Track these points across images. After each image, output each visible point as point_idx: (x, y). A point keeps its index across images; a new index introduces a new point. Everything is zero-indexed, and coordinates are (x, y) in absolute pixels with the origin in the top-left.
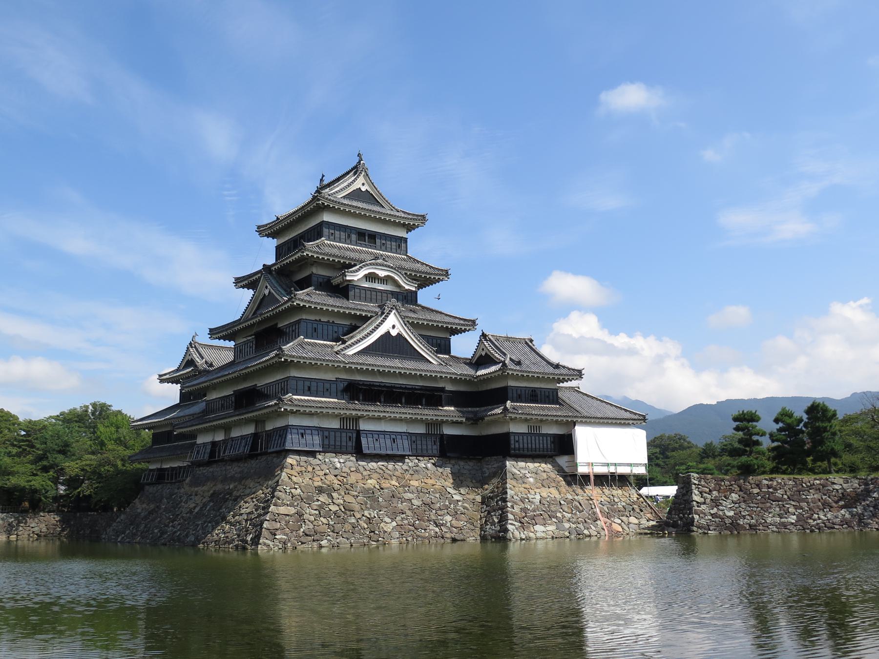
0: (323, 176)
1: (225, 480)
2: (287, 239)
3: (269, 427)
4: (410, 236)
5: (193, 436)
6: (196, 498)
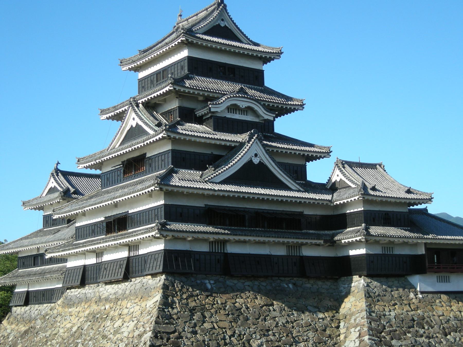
4: (267, 68)
5: (63, 260)
6: (72, 318)
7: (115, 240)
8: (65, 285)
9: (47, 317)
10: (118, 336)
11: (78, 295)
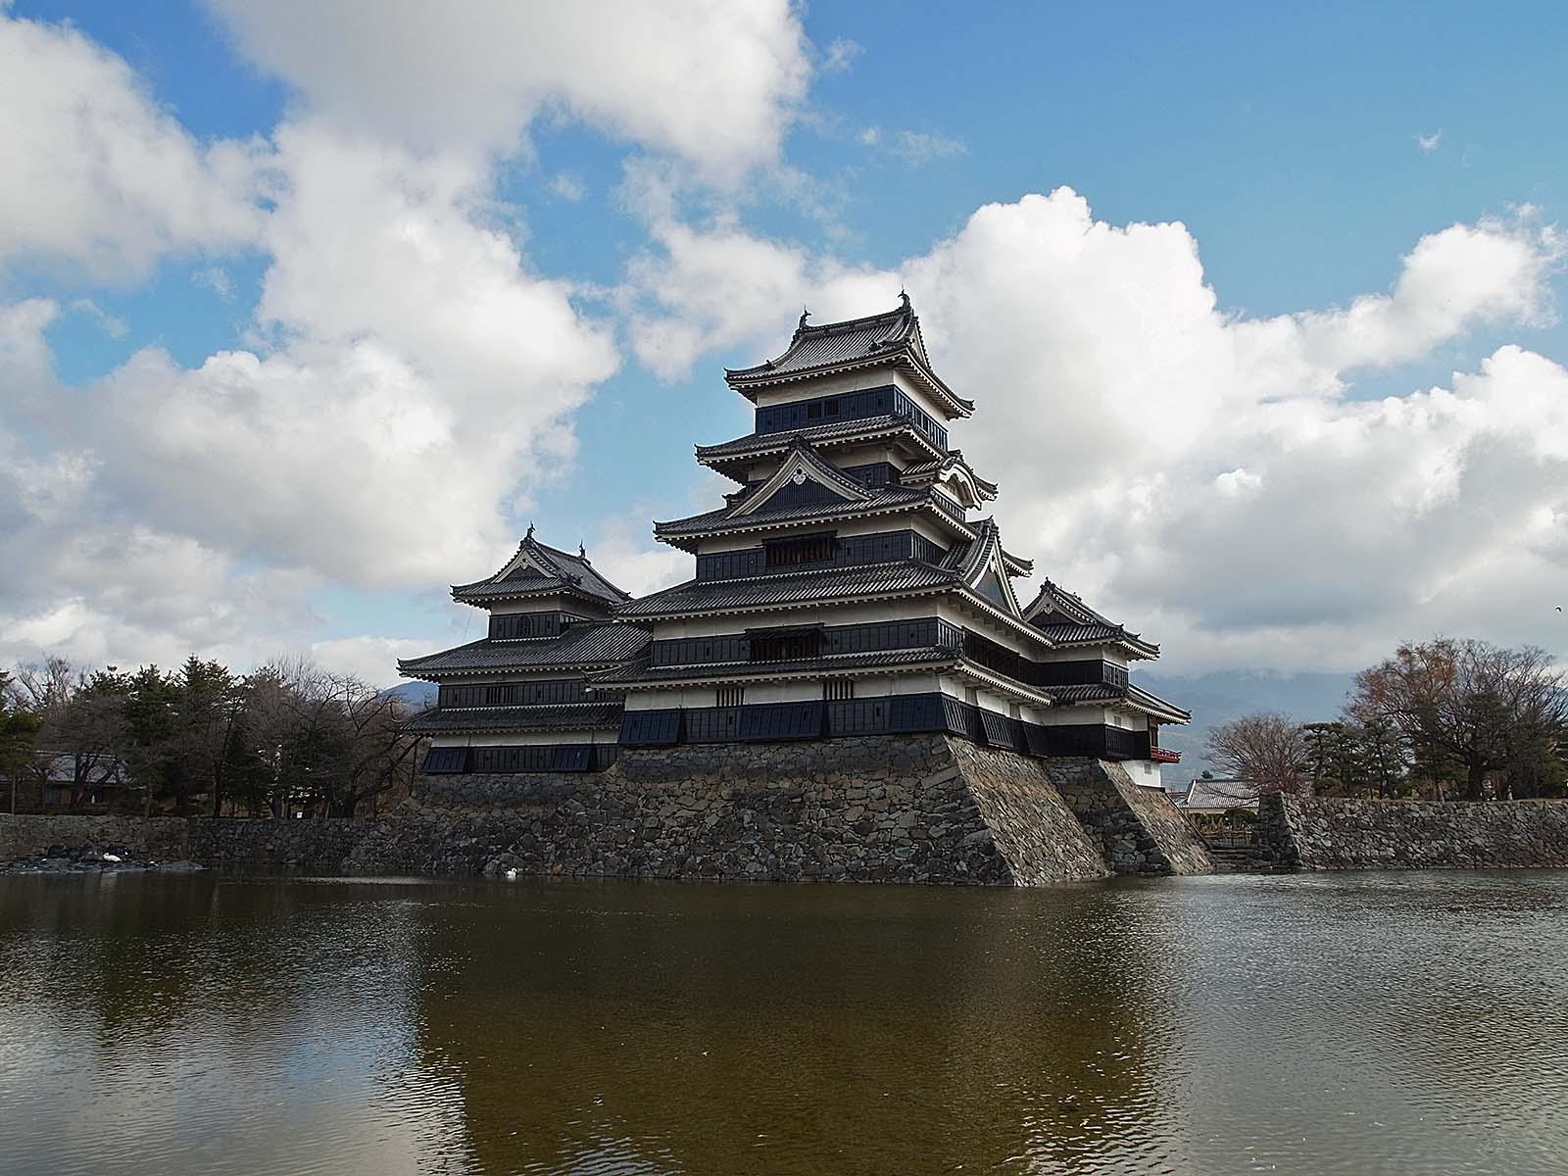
0: (806, 314)
1: (745, 773)
2: (789, 401)
3: (863, 692)
4: (951, 426)
5: (623, 695)
7: (820, 670)
9: (598, 797)
10: (873, 835)
11: (669, 761)
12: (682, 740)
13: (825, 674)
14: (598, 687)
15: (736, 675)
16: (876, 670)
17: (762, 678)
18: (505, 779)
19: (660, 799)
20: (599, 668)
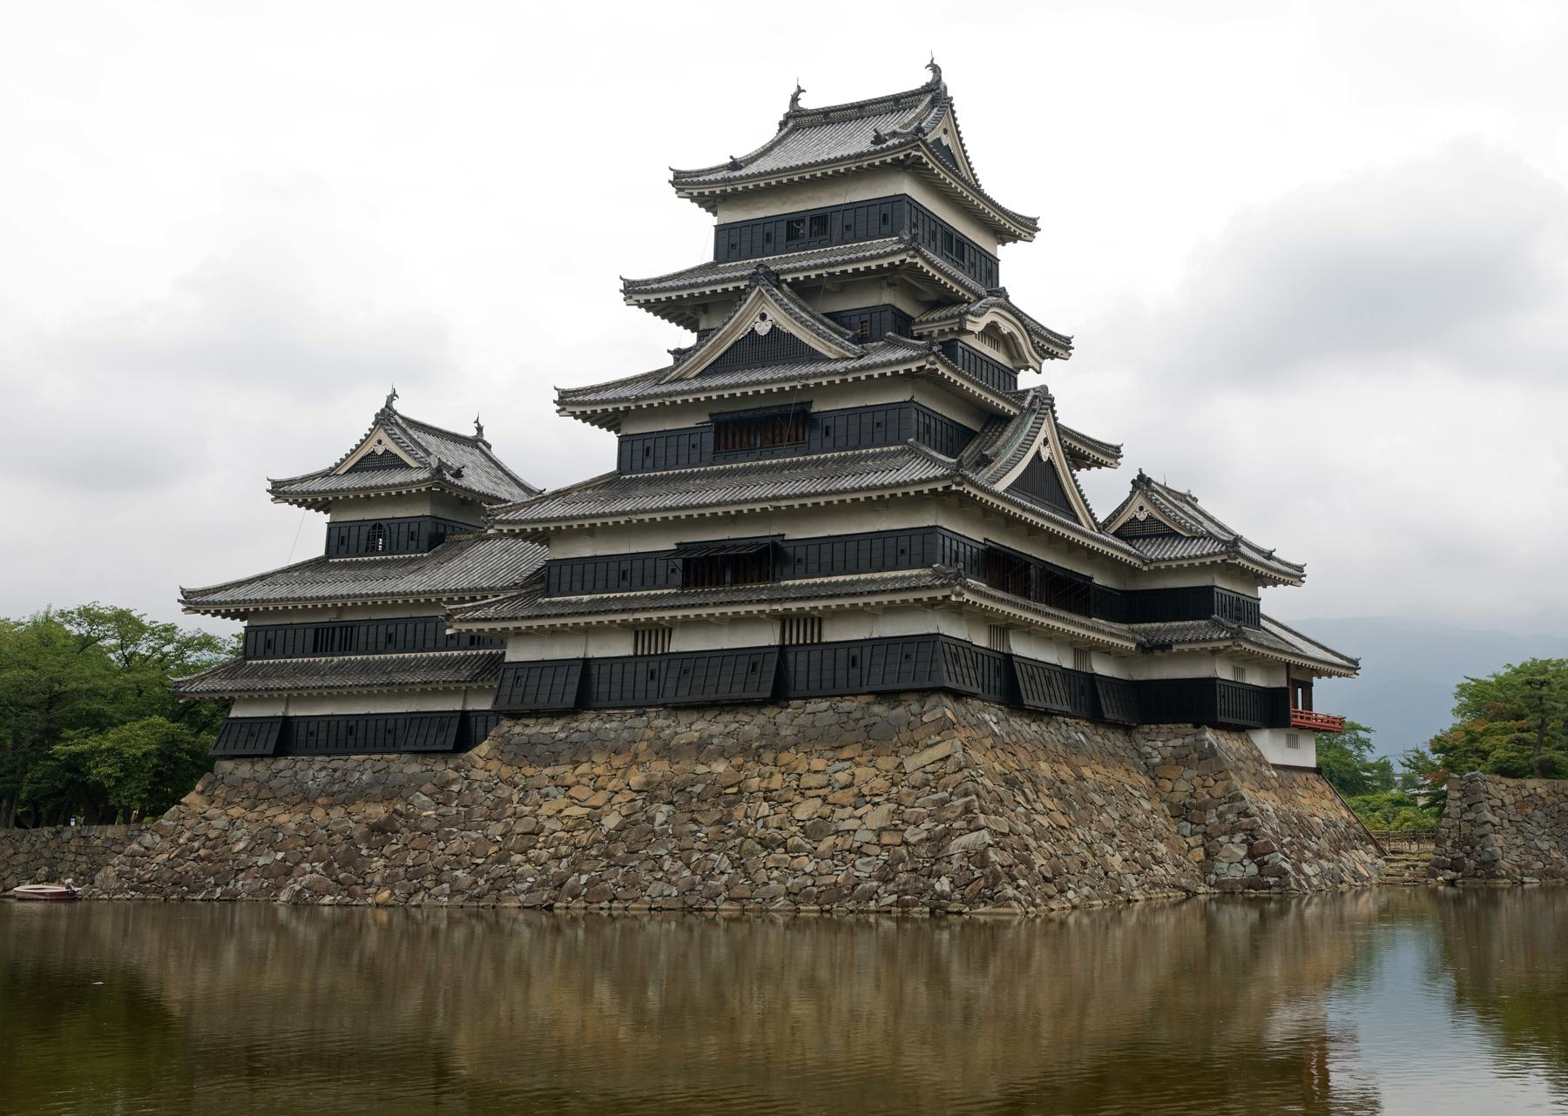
1: (667, 751)
3: (834, 633)
5: (500, 639)
7: (771, 601)
8: (505, 707)
11: (562, 735)
12: (584, 702)
13: (779, 607)
14: (464, 627)
15: (656, 609)
16: (847, 602)
17: (692, 613)
18: (335, 764)
19: (543, 791)
20: (462, 600)
